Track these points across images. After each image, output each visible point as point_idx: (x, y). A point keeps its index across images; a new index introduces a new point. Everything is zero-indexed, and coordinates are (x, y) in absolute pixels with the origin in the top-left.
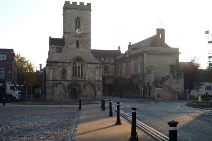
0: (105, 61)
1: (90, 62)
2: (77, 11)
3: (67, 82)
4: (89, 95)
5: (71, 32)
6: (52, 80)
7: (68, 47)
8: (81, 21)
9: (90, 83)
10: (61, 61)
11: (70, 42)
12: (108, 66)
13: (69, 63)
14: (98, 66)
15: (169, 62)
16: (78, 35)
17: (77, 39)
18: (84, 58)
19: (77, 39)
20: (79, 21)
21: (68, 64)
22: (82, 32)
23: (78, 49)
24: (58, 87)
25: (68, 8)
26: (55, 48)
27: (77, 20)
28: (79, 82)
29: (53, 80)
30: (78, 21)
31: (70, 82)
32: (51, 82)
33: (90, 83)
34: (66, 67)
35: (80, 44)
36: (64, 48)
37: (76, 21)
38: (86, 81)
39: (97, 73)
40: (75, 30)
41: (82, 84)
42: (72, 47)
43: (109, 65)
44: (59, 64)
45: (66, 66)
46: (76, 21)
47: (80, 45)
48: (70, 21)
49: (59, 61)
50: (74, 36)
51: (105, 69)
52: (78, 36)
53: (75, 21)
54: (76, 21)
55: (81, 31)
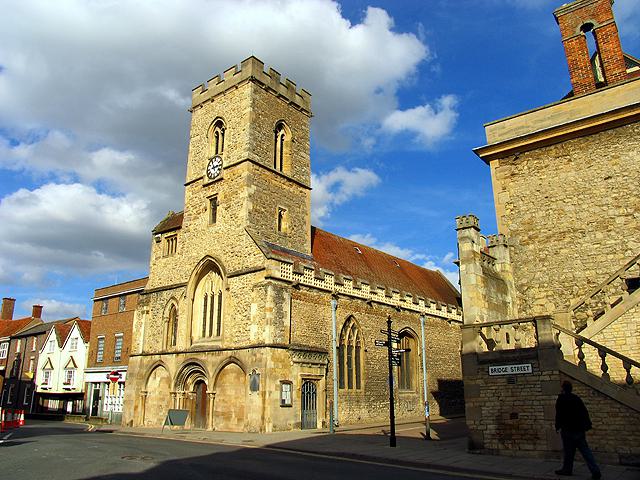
1: (238, 268)
6: (141, 352)
10: (171, 283)
19: (211, 193)
23: (213, 229)
24: (158, 379)
26: (164, 242)
36: (180, 234)
39: (254, 307)
41: (211, 362)
44: (165, 293)
45: (178, 298)
49: (166, 284)
50: (204, 186)
54: (217, 132)
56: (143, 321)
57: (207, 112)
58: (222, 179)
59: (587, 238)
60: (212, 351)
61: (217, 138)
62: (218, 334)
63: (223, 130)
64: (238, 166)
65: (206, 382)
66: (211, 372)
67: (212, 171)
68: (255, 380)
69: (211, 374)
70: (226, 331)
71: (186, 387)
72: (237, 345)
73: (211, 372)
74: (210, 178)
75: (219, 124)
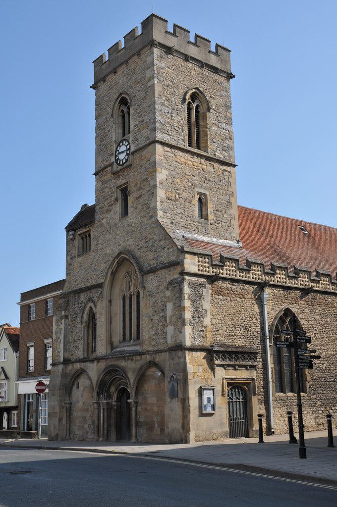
4: (155, 420)
6: (62, 360)
7: (101, 225)
13: (100, 286)
16: (123, 164)
19: (121, 181)
21: (99, 290)
23: (126, 222)
24: (81, 388)
28: (123, 364)
29: (64, 360)
31: (103, 365)
32: (61, 367)
34: (95, 306)
47: (130, 199)
49: (82, 286)
54: (123, 111)
56: (62, 326)
57: (111, 88)
58: (131, 165)
61: (123, 117)
62: (138, 338)
63: (129, 108)
65: (129, 390)
66: (132, 378)
67: (122, 157)
68: (173, 387)
69: (132, 381)
70: (145, 334)
71: (109, 396)
72: (155, 349)
73: (132, 378)
74: (119, 164)
75: (123, 102)
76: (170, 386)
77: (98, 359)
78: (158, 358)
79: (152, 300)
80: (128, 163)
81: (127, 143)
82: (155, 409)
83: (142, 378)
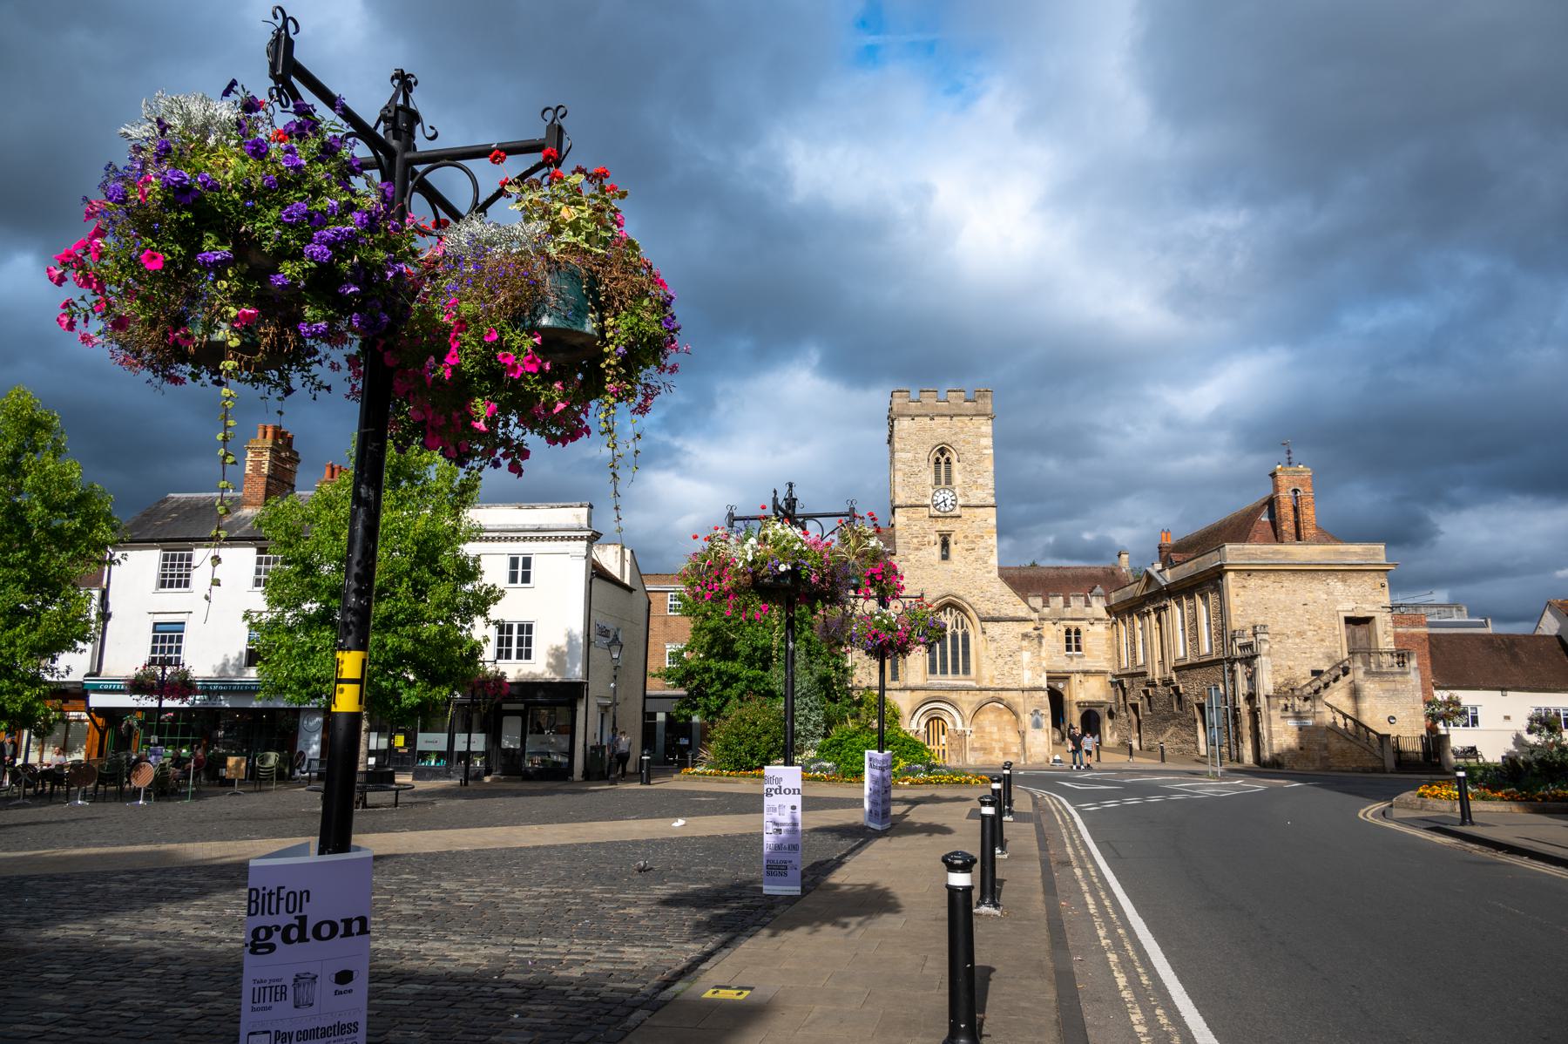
0: (1068, 612)
1: (996, 614)
2: (938, 420)
3: (909, 692)
5: (918, 503)
7: (908, 561)
8: (954, 459)
9: (999, 701)
11: (915, 540)
12: (1078, 632)
14: (1028, 628)
15: (1339, 608)
16: (945, 512)
17: (943, 529)
18: (970, 600)
20: (948, 459)
22: (961, 501)
23: (946, 565)
25: (903, 416)
27: (938, 455)
30: (943, 460)
31: (922, 695)
33: (999, 701)
35: (952, 546)
37: (938, 459)
38: (980, 690)
40: (934, 495)
42: (922, 560)
43: (1083, 626)
46: (937, 462)
48: (914, 464)
51: (1068, 640)
52: (947, 517)
53: (932, 460)
54: (938, 459)
55: (954, 494)
58: (960, 517)
59: (1290, 641)
60: (968, 689)
64: (981, 510)
68: (1037, 720)
72: (1000, 686)
74: (939, 510)
76: (1034, 718)
77: (913, 690)
78: (1004, 694)
79: (995, 644)
80: (952, 513)
81: (951, 494)
82: (996, 736)
83: (979, 709)
